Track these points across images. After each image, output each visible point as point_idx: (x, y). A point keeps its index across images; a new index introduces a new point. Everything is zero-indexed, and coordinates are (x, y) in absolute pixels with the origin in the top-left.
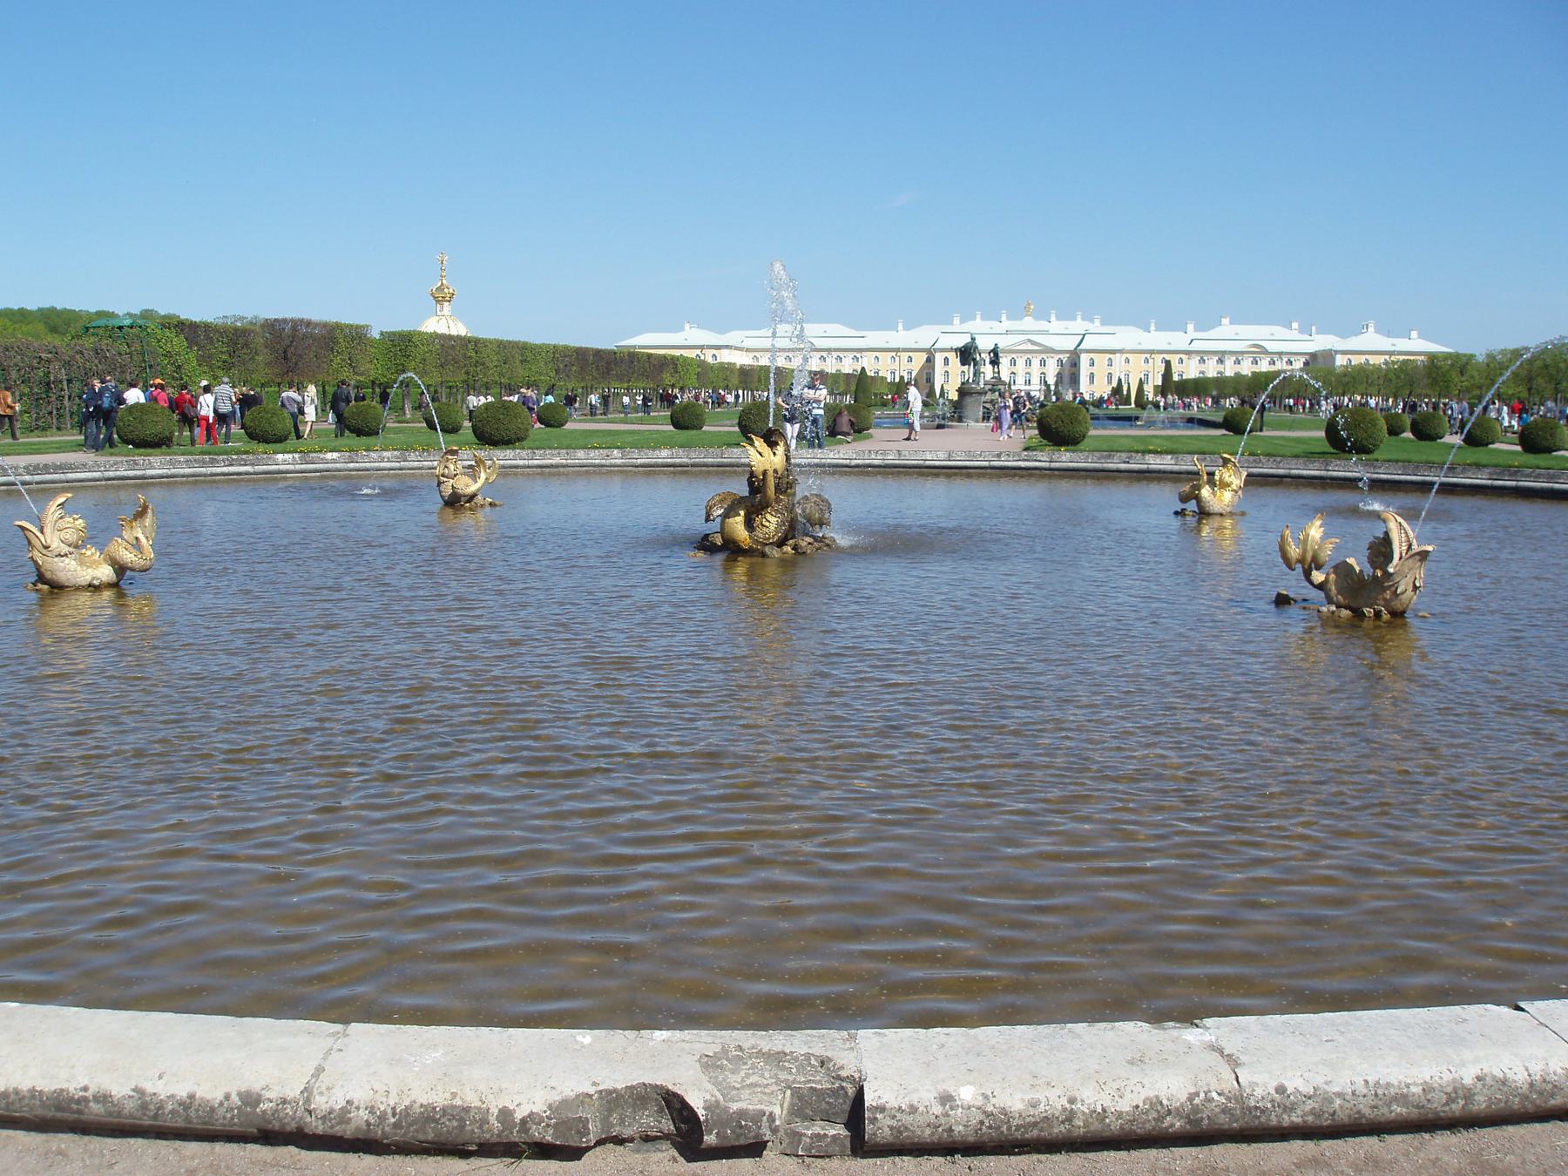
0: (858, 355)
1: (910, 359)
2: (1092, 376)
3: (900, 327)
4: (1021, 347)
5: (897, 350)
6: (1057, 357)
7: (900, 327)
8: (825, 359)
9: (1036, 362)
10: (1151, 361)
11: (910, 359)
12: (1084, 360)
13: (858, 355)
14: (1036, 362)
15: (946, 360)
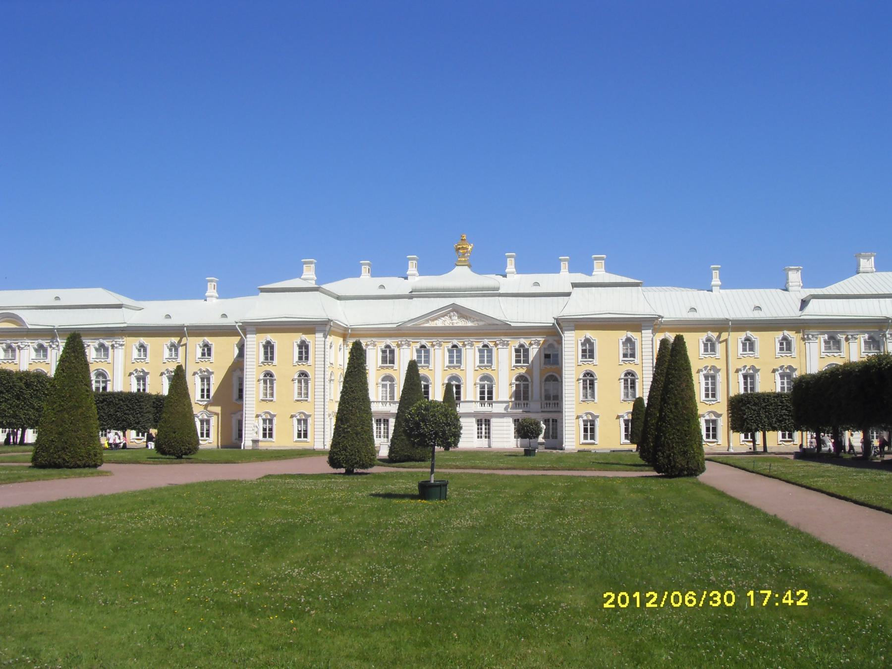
0: (107, 343)
1: (207, 350)
2: (589, 381)
3: (211, 291)
4: (439, 323)
5: (179, 331)
6: (515, 343)
7: (211, 291)
8: (45, 350)
9: (471, 355)
10: (720, 348)
11: (207, 350)
12: (571, 342)
13: (107, 343)
14: (471, 355)
15: (269, 348)
